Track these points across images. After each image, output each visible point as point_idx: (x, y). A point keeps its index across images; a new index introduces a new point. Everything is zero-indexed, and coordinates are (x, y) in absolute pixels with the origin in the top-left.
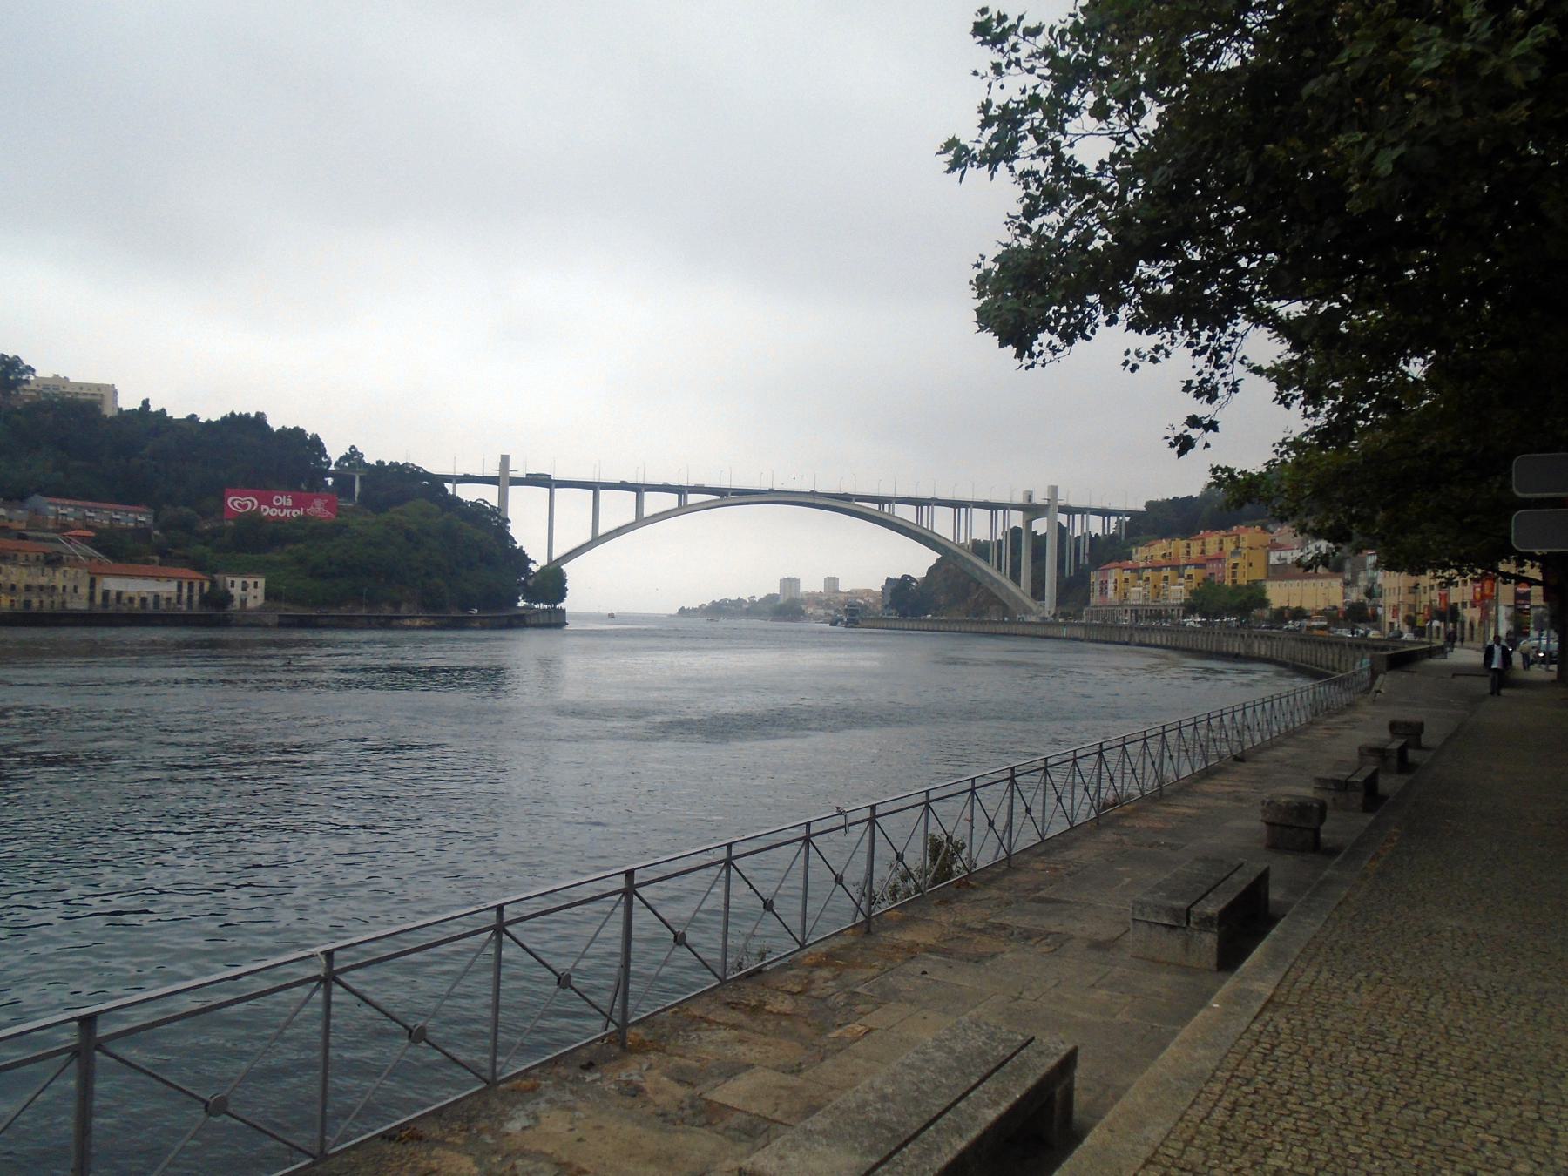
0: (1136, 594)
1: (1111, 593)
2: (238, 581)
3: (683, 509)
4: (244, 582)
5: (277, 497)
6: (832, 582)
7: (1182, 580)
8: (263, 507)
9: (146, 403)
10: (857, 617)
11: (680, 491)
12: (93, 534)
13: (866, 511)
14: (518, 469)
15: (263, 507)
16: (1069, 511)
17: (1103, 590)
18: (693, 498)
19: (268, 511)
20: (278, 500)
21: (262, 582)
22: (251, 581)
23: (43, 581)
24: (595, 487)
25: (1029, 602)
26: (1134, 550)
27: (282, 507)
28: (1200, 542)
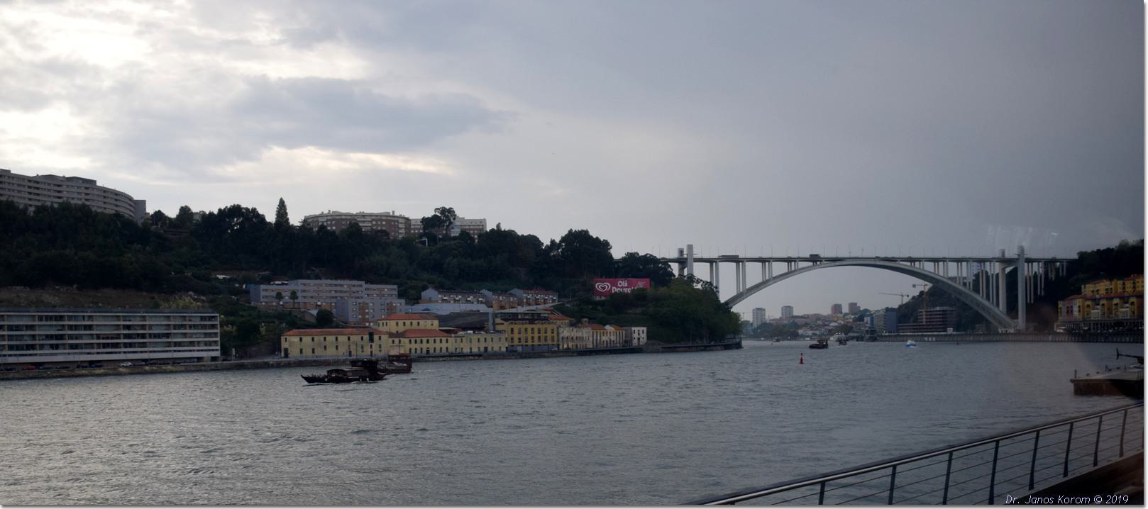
0: (1096, 313)
1: (1076, 313)
2: (636, 329)
4: (639, 331)
5: (620, 282)
6: (787, 309)
7: (1127, 305)
8: (613, 288)
9: (498, 226)
10: (875, 335)
11: (789, 260)
14: (698, 253)
15: (613, 288)
16: (1029, 261)
17: (1070, 311)
18: (802, 265)
19: (615, 290)
20: (620, 284)
21: (645, 329)
23: (580, 335)
25: (1008, 319)
26: (1083, 286)
27: (622, 287)
28: (1132, 282)
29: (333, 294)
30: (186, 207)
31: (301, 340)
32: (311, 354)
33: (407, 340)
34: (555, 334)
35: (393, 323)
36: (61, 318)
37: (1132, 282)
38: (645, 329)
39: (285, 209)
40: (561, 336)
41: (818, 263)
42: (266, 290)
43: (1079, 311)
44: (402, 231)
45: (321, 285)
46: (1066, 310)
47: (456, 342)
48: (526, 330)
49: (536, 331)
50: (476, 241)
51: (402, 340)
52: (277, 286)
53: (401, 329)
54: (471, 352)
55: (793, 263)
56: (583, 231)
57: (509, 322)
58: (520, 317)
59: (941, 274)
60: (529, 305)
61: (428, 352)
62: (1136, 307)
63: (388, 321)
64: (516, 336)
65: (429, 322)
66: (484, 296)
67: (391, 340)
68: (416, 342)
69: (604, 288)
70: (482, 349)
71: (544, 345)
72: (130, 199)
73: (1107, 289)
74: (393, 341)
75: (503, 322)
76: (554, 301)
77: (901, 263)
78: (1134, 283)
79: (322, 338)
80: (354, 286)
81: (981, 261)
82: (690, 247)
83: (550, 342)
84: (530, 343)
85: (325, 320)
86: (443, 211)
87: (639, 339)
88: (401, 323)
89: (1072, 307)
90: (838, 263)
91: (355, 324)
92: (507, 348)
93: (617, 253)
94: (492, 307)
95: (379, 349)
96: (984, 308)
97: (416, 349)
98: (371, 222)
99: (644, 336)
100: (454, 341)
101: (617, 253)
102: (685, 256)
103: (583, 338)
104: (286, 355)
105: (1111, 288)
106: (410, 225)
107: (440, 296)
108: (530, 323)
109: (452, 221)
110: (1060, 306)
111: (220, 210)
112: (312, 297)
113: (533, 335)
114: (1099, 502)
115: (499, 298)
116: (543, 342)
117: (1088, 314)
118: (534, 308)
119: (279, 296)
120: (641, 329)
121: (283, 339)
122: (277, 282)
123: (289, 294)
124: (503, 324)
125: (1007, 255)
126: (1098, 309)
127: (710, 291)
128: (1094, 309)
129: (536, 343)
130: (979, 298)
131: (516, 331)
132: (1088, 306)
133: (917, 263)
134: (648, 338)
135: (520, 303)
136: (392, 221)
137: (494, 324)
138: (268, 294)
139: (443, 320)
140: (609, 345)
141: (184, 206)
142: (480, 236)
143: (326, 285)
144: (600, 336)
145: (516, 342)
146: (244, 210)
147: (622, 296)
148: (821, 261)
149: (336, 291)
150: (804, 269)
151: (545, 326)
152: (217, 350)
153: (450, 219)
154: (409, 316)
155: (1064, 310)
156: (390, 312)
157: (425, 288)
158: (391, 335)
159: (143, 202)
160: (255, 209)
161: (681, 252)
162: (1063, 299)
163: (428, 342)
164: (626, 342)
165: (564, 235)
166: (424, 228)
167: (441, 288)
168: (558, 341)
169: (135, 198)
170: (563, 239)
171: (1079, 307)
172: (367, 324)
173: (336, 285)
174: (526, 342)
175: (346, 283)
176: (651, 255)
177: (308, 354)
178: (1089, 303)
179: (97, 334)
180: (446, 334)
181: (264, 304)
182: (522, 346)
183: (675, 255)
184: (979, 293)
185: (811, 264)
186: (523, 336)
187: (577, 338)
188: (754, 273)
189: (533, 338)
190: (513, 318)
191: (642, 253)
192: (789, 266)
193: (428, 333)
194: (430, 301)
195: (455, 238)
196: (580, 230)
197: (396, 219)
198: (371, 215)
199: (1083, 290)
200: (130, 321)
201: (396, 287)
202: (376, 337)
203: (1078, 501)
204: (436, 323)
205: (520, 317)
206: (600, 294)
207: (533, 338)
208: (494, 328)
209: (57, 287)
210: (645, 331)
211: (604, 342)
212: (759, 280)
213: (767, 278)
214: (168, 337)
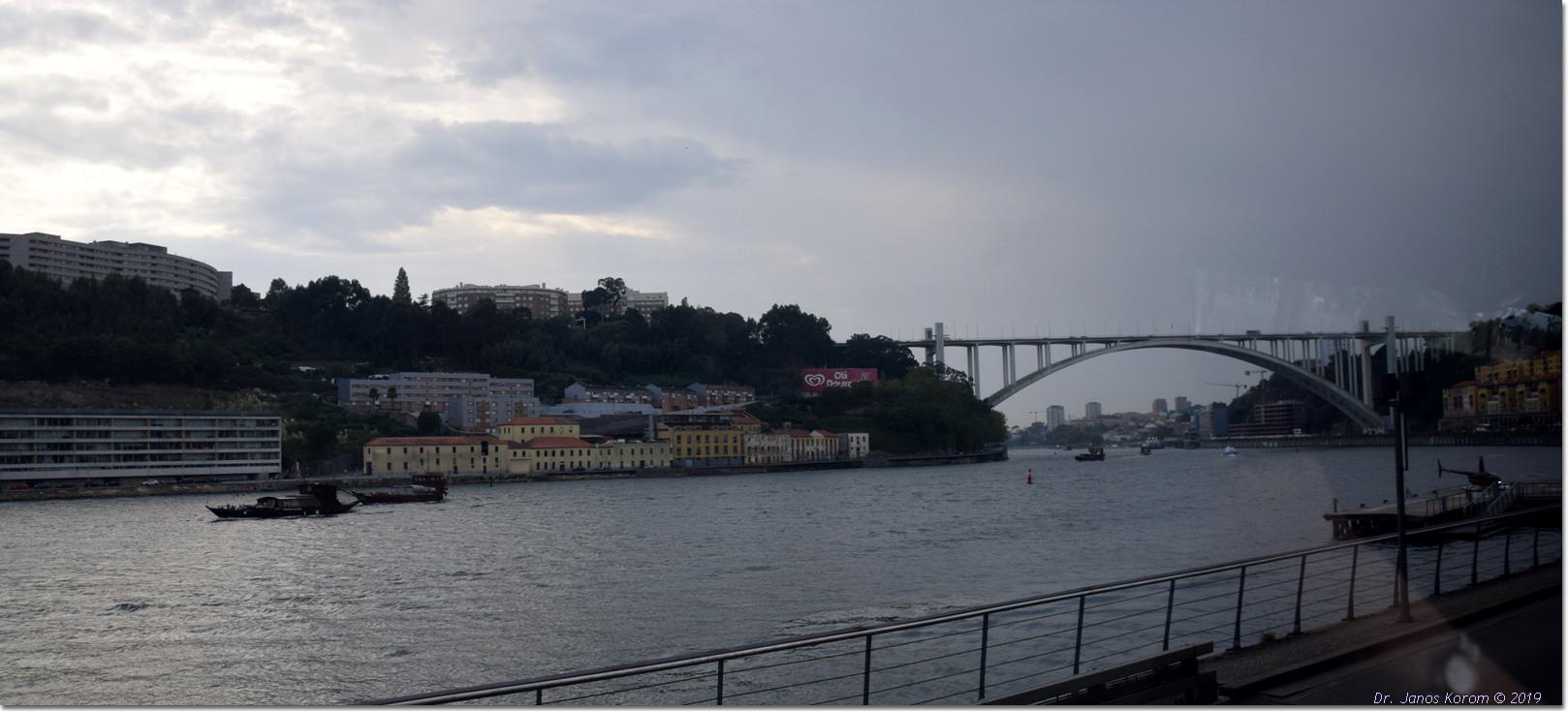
0: (1494, 405)
1: (1467, 406)
2: (854, 435)
3: (1073, 359)
4: (858, 438)
7: (1536, 393)
10: (1198, 440)
11: (1072, 342)
12: (1402, 415)
13: (1227, 347)
15: (829, 381)
16: (1400, 336)
17: (1458, 403)
18: (1090, 347)
19: (831, 383)
20: (838, 376)
21: (867, 435)
22: (861, 435)
23: (774, 444)
24: (1004, 344)
26: (1476, 369)
27: (841, 380)
28: (1542, 361)
29: (447, 391)
30: (281, 280)
31: (389, 451)
32: (402, 470)
33: (534, 452)
34: (739, 444)
35: (518, 429)
36: (68, 422)
37: (1542, 361)
38: (867, 435)
39: (406, 282)
40: (746, 446)
41: (1113, 344)
42: (358, 386)
43: (1471, 403)
44: (556, 309)
45: (431, 379)
46: (1453, 402)
47: (601, 454)
48: (698, 438)
49: (712, 440)
50: (649, 321)
51: (527, 451)
52: (380, 382)
53: (528, 436)
54: (622, 467)
55: (1078, 346)
56: (791, 306)
57: (675, 427)
58: (691, 420)
59: (1281, 356)
60: (714, 404)
61: (562, 467)
62: (1548, 396)
63: (511, 427)
64: (684, 445)
65: (566, 428)
66: (650, 393)
67: (512, 451)
68: (546, 455)
70: (637, 464)
71: (724, 458)
72: (211, 270)
73: (1509, 372)
74: (515, 454)
75: (667, 427)
76: (748, 399)
77: (1226, 342)
78: (1545, 363)
79: (417, 449)
80: (475, 380)
81: (1337, 338)
82: (939, 326)
83: (731, 454)
84: (703, 455)
85: (429, 425)
86: (610, 282)
87: (858, 449)
88: (528, 428)
89: (1461, 397)
90: (1139, 344)
91: (471, 430)
92: (671, 462)
93: (839, 335)
94: (661, 407)
95: (495, 463)
96: (1342, 401)
97: (546, 464)
98: (514, 297)
99: (865, 446)
100: (598, 453)
101: (839, 335)
102: (934, 338)
103: (778, 448)
104: (370, 472)
105: (1515, 371)
106: (566, 301)
107: (588, 393)
108: (703, 429)
109: (621, 295)
110: (1445, 396)
111: (311, 283)
112: (418, 395)
113: (707, 445)
114: (1501, 702)
115: (670, 395)
116: (721, 454)
117: (1483, 407)
118: (709, 408)
119: (374, 394)
120: (861, 435)
121: (366, 449)
122: (377, 376)
123: (385, 391)
124: (666, 430)
126: (1496, 400)
128: (1491, 400)
129: (712, 454)
130: (1334, 388)
131: (684, 439)
132: (1483, 396)
133: (1247, 343)
134: (872, 447)
135: (702, 402)
136: (542, 296)
137: (656, 430)
138: (358, 392)
139: (586, 424)
140: (816, 457)
141: (277, 278)
142: (654, 314)
143: (438, 380)
144: (803, 446)
145: (684, 453)
146: (341, 284)
147: (839, 392)
148: (1116, 342)
149: (451, 387)
150: (1092, 354)
151: (724, 433)
152: (277, 464)
153: (618, 293)
154: (543, 419)
155: (1451, 401)
156: (520, 412)
157: (571, 382)
158: (512, 445)
159: (229, 275)
160: (357, 281)
161: (929, 332)
162: (1449, 386)
163: (562, 453)
164: (840, 453)
165: (766, 313)
166: (585, 305)
167: (595, 383)
168: (742, 452)
169: (219, 270)
170: (765, 318)
171: (1471, 396)
172: (488, 431)
173: (451, 380)
174: (698, 454)
175: (465, 377)
176: (886, 338)
177: (398, 471)
178: (1483, 391)
179: (115, 443)
180: (589, 444)
181: (354, 403)
182: (693, 459)
183: (921, 337)
184: (1334, 382)
185: (1103, 346)
186: (694, 445)
187: (769, 448)
188: (1026, 360)
189: (707, 448)
190: (681, 422)
191: (873, 336)
192: (1074, 350)
193: (565, 442)
194: (576, 399)
195: (621, 318)
196: (788, 305)
197: (547, 293)
198: (513, 289)
199: (1477, 374)
200: (160, 425)
201: (531, 381)
202: (491, 448)
203: (1473, 699)
204: (576, 428)
205: (691, 420)
206: (812, 389)
207: (707, 448)
208: (656, 434)
209: (84, 382)
210: (867, 439)
211: (808, 453)
212: (1035, 369)
213: (1044, 366)
214: (211, 448)
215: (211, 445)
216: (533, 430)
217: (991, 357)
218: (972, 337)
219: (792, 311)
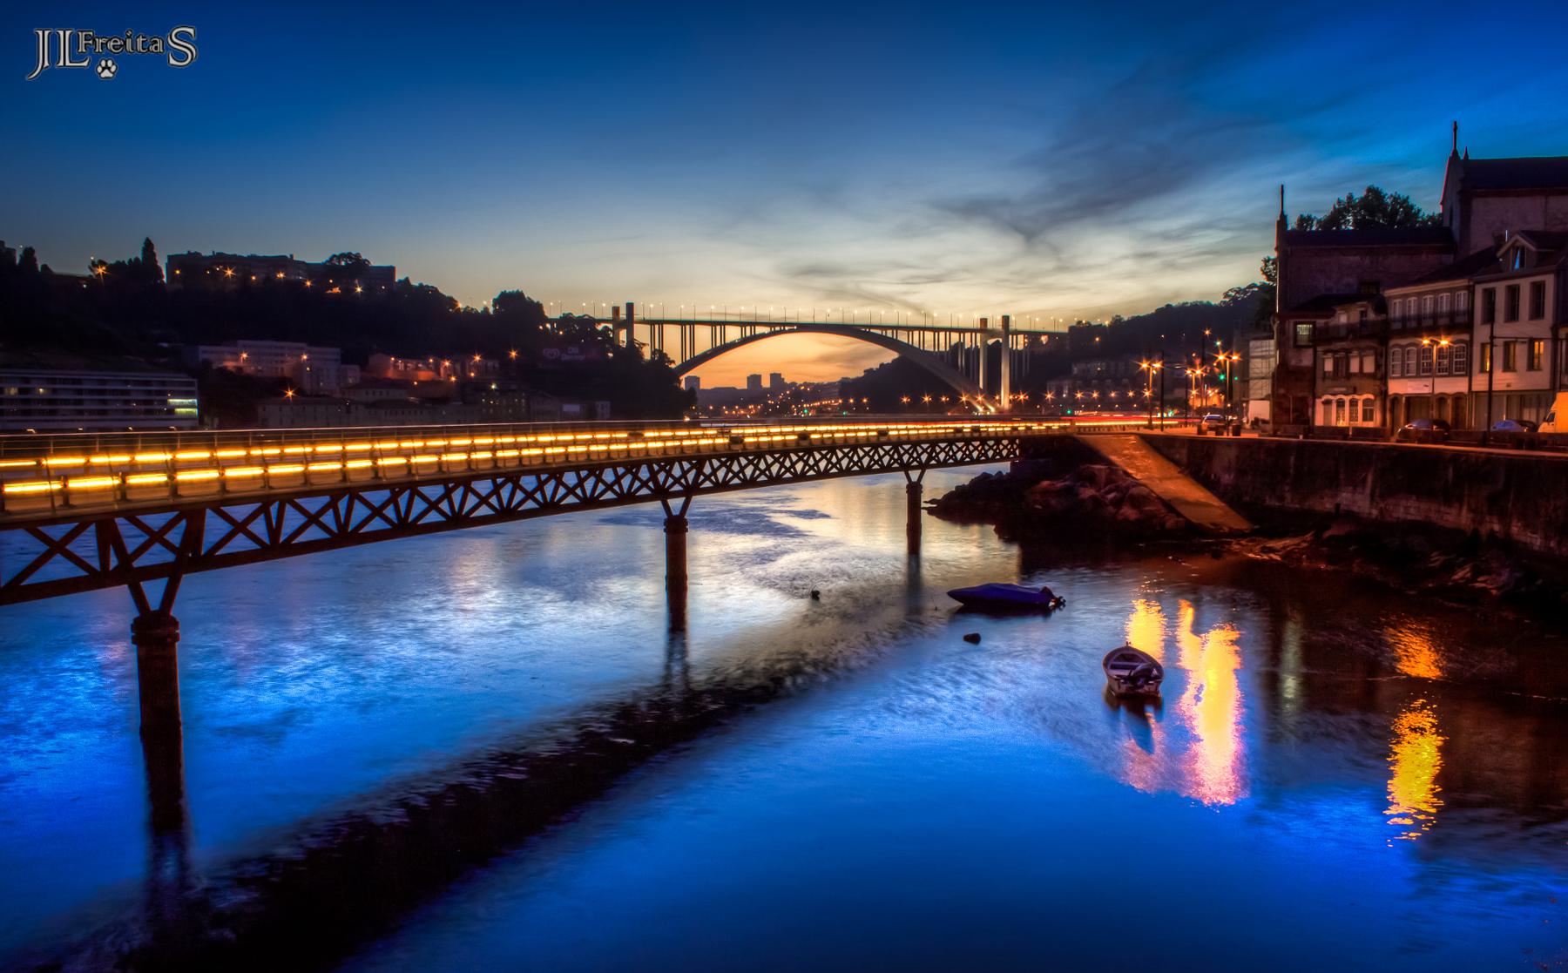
3: (745, 341)
11: (742, 324)
18: (760, 330)
19: (565, 357)
21: (608, 403)
38: (608, 403)
59: (916, 345)
69: (552, 355)
77: (872, 331)
82: (630, 307)
125: (989, 326)
127: (661, 357)
150: (763, 336)
161: (616, 310)
173: (276, 347)
185: (766, 330)
210: (609, 405)
215: (79, 402)
216: (381, 393)
217: (672, 335)
218: (657, 316)
219: (519, 295)
